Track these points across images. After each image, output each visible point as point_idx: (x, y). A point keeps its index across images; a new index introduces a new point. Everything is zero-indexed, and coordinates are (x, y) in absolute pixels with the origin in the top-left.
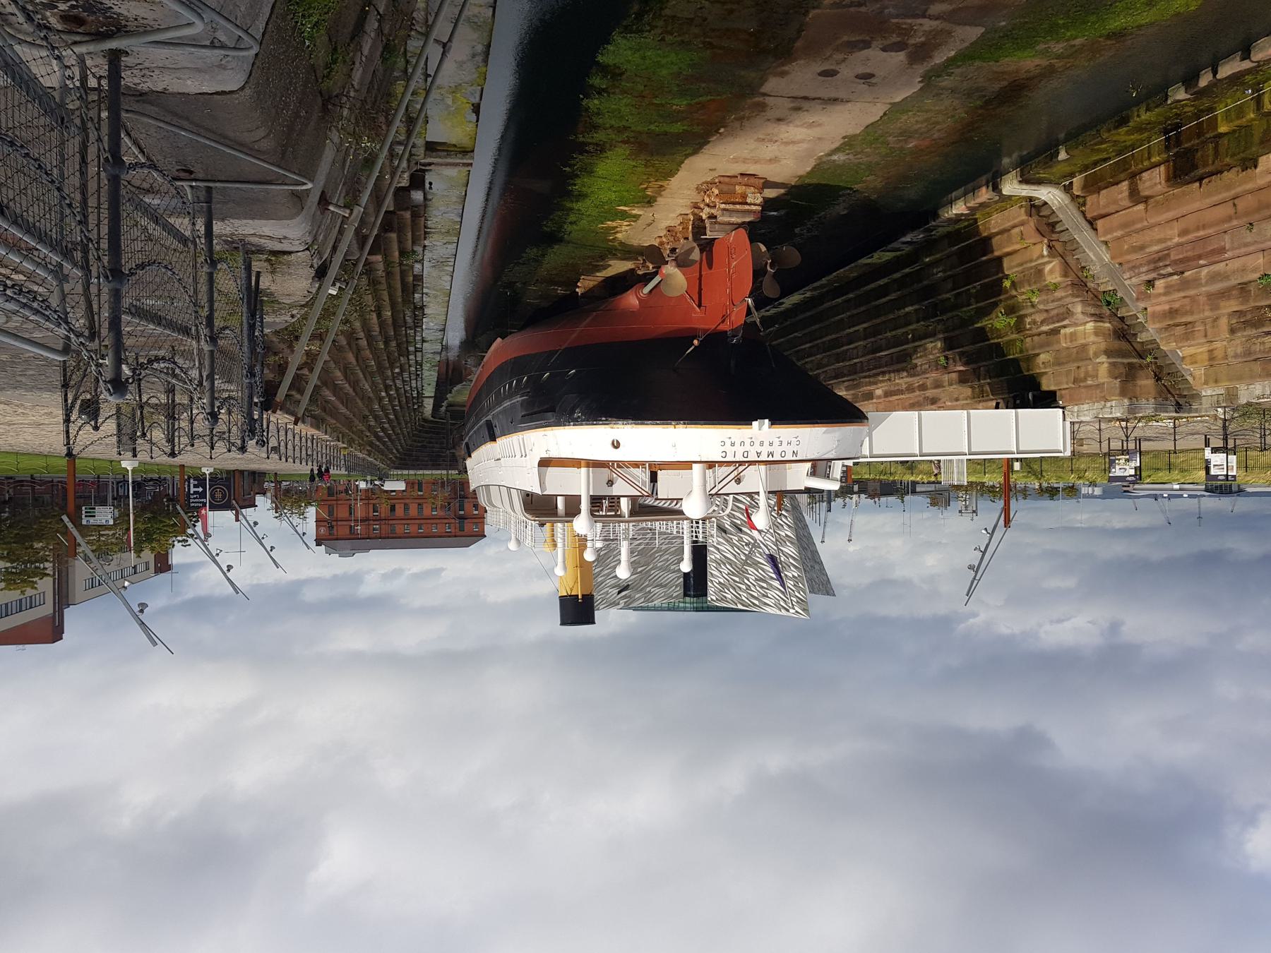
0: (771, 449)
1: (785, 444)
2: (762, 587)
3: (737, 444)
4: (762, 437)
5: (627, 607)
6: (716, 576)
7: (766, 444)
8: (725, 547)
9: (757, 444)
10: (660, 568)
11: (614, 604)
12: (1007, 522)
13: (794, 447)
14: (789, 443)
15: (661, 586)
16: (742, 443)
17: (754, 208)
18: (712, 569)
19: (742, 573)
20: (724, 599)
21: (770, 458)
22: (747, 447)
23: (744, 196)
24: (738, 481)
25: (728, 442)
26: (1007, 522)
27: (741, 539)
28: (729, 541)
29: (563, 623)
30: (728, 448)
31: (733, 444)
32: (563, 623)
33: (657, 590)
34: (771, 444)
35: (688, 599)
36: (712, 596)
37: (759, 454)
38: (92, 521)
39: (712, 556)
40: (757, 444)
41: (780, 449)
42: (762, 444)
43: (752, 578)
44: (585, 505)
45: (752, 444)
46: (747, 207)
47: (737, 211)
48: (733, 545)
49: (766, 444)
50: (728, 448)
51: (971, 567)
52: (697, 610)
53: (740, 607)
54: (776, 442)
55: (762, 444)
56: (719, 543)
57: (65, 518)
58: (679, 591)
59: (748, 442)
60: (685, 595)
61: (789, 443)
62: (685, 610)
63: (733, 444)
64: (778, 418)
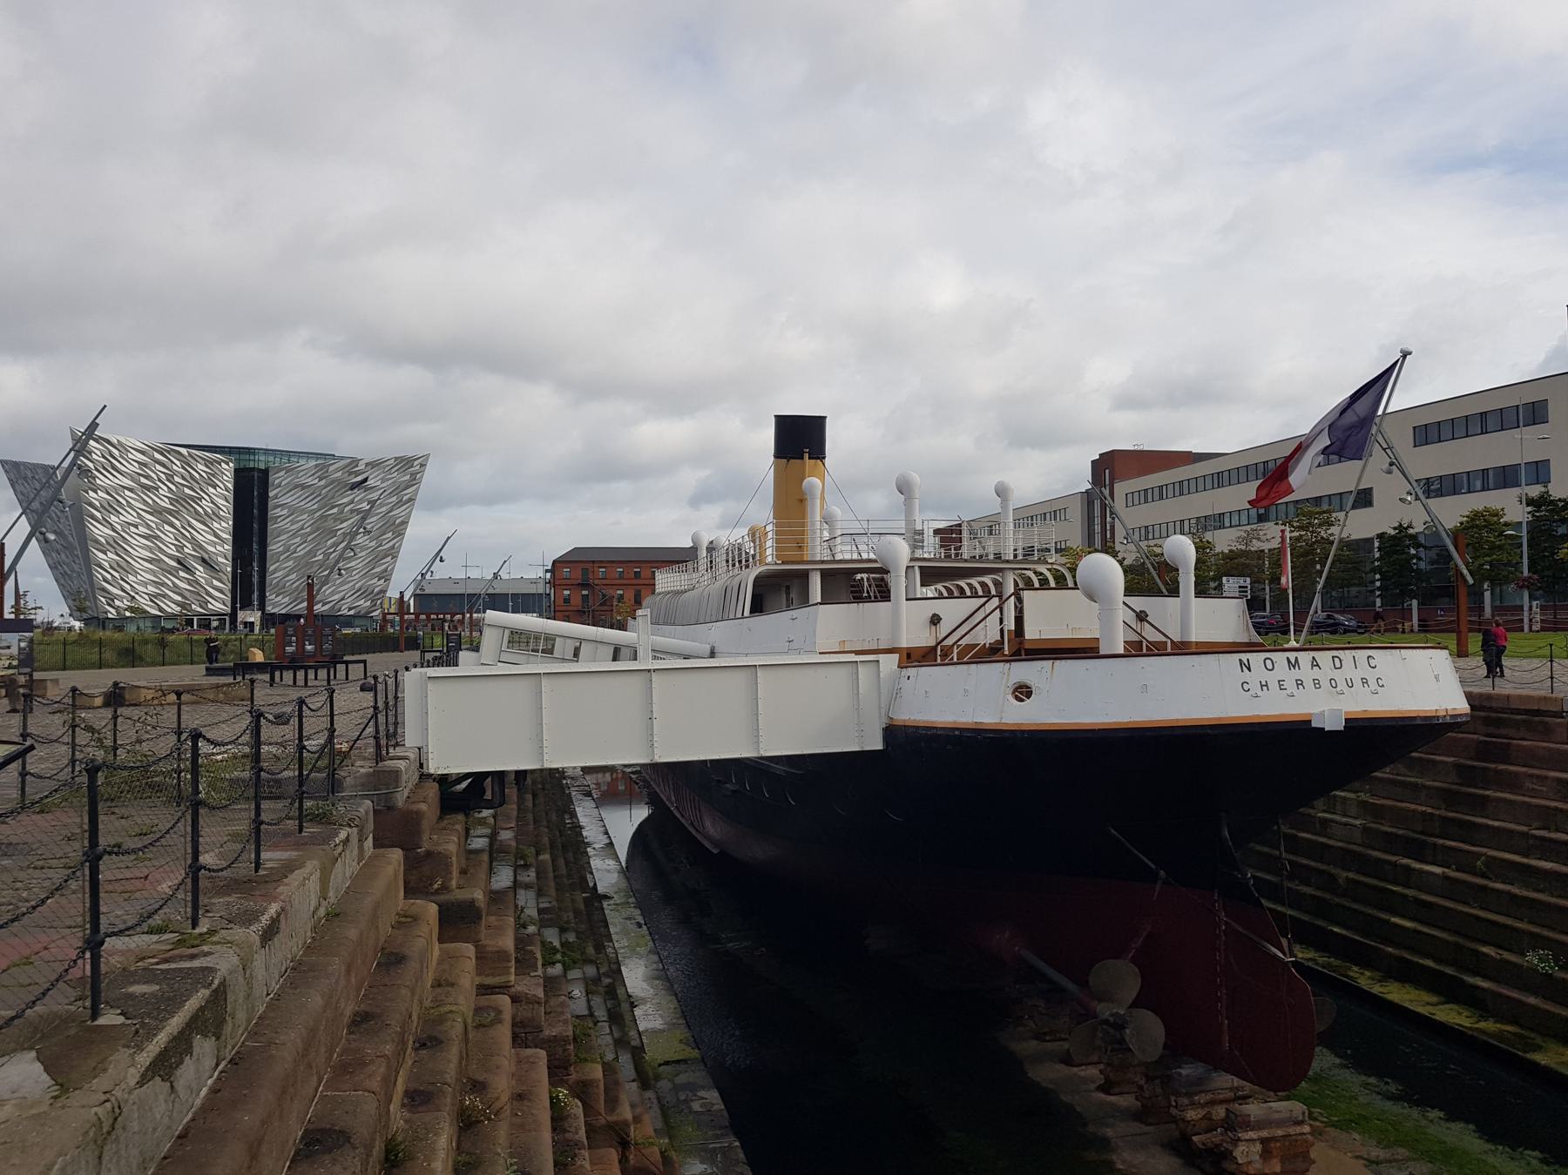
0: (1295, 674)
1: (1273, 685)
3: (1357, 683)
5: (355, 462)
6: (220, 497)
7: (1308, 684)
8: (204, 537)
9: (1325, 684)
10: (303, 512)
11: (372, 465)
15: (303, 487)
17: (1252, 1135)
18: (226, 508)
19: (179, 500)
23: (1266, 1154)
24: (935, 620)
27: (180, 548)
28: (197, 545)
29: (820, 421)
31: (1364, 681)
32: (820, 421)
33: (310, 481)
34: (1299, 683)
35: (262, 466)
36: (227, 470)
37: (1315, 664)
38: (1241, 581)
39: (225, 527)
40: (1325, 684)
43: (164, 491)
44: (1188, 581)
46: (1265, 1134)
47: (1280, 1123)
49: (1308, 684)
50: (1371, 676)
52: (249, 451)
54: (1290, 685)
56: (214, 544)
57: (1471, 581)
58: (276, 478)
59: (1342, 686)
60: (265, 473)
62: (267, 451)
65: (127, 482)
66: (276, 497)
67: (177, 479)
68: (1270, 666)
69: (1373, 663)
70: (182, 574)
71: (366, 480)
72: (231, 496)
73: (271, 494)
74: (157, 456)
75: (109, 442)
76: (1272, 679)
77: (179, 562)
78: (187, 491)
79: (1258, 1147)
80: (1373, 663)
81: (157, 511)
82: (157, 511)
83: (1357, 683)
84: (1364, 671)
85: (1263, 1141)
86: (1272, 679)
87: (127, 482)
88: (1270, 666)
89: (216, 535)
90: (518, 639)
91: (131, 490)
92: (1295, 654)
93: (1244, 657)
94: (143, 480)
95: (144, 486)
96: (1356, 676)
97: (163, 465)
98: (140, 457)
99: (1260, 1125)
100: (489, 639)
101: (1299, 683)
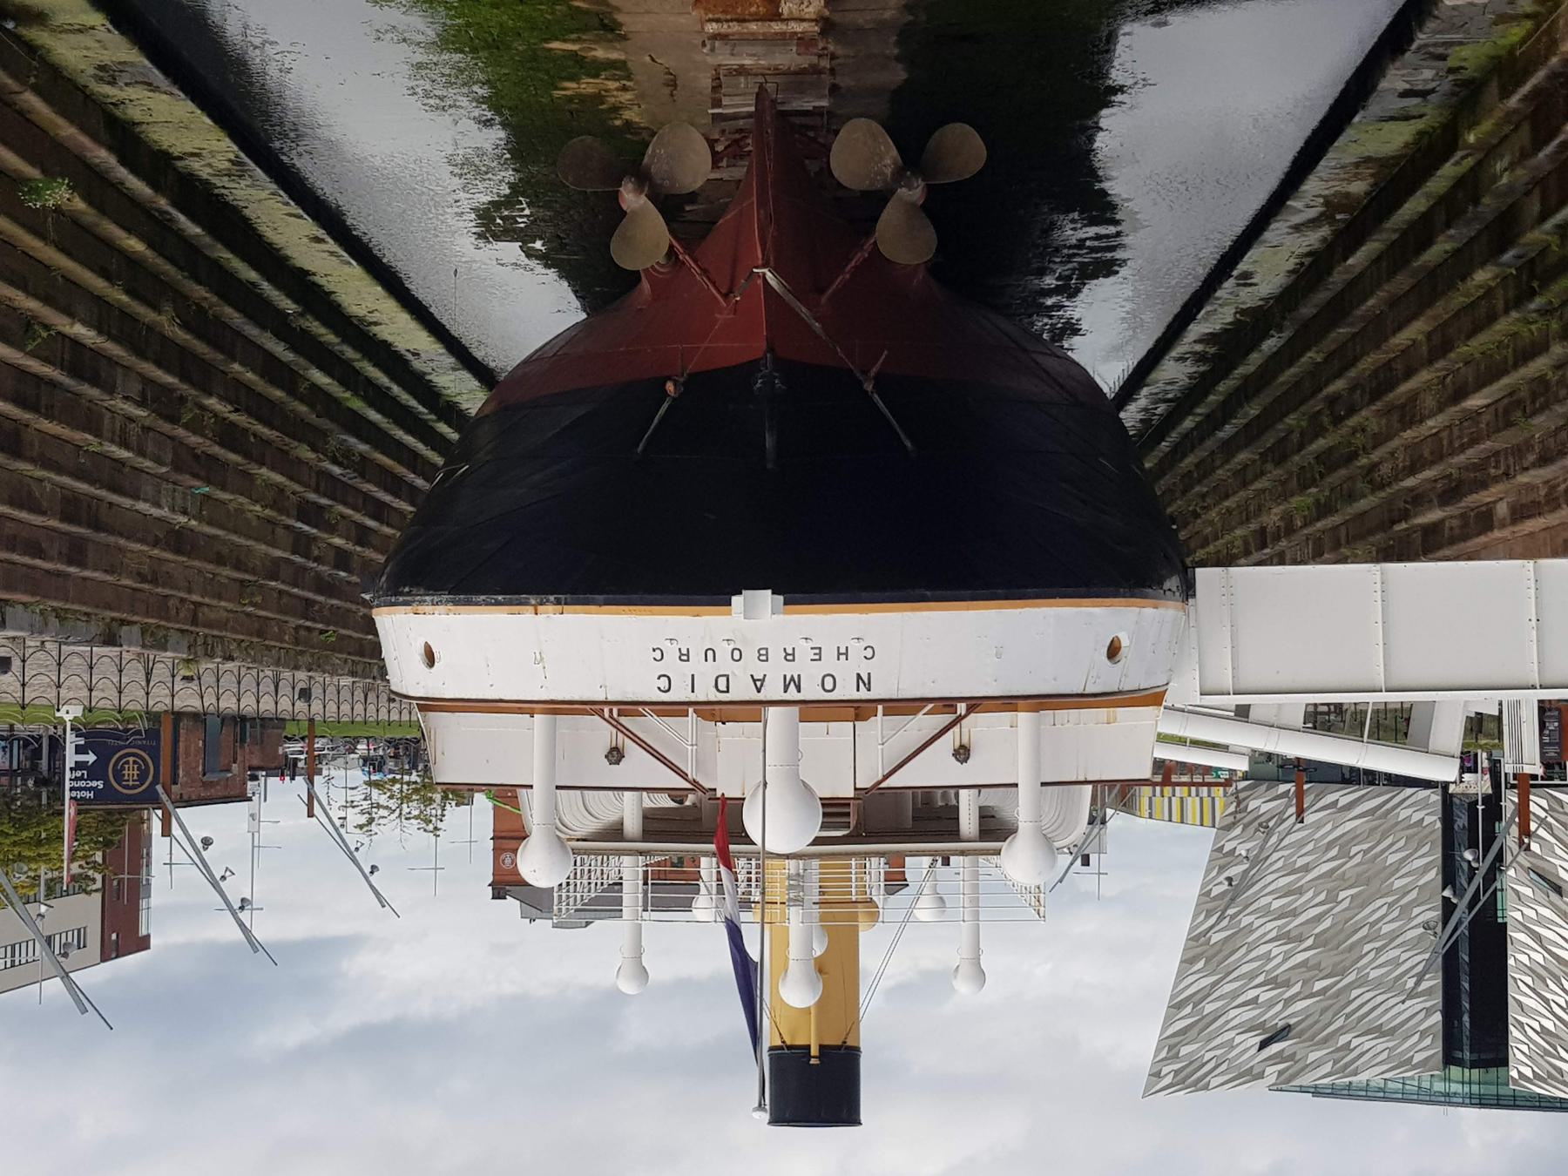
0: (791, 670)
1: (829, 654)
3: (697, 656)
4: (755, 635)
7: (776, 655)
9: (750, 655)
14: (843, 654)
16: (710, 654)
21: (792, 694)
22: (724, 664)
25: (671, 652)
30: (671, 665)
34: (790, 656)
37: (759, 684)
40: (750, 655)
41: (819, 669)
42: (763, 655)
45: (737, 655)
49: (776, 655)
50: (671, 665)
54: (804, 652)
55: (763, 655)
59: (724, 651)
61: (843, 654)
63: (685, 657)
64: (805, 584)
68: (829, 681)
69: (663, 683)
76: (829, 663)
83: (697, 656)
84: (680, 673)
86: (829, 663)
88: (829, 681)
90: (1395, 726)
92: (787, 697)
93: (863, 694)
96: (696, 664)
101: (790, 656)
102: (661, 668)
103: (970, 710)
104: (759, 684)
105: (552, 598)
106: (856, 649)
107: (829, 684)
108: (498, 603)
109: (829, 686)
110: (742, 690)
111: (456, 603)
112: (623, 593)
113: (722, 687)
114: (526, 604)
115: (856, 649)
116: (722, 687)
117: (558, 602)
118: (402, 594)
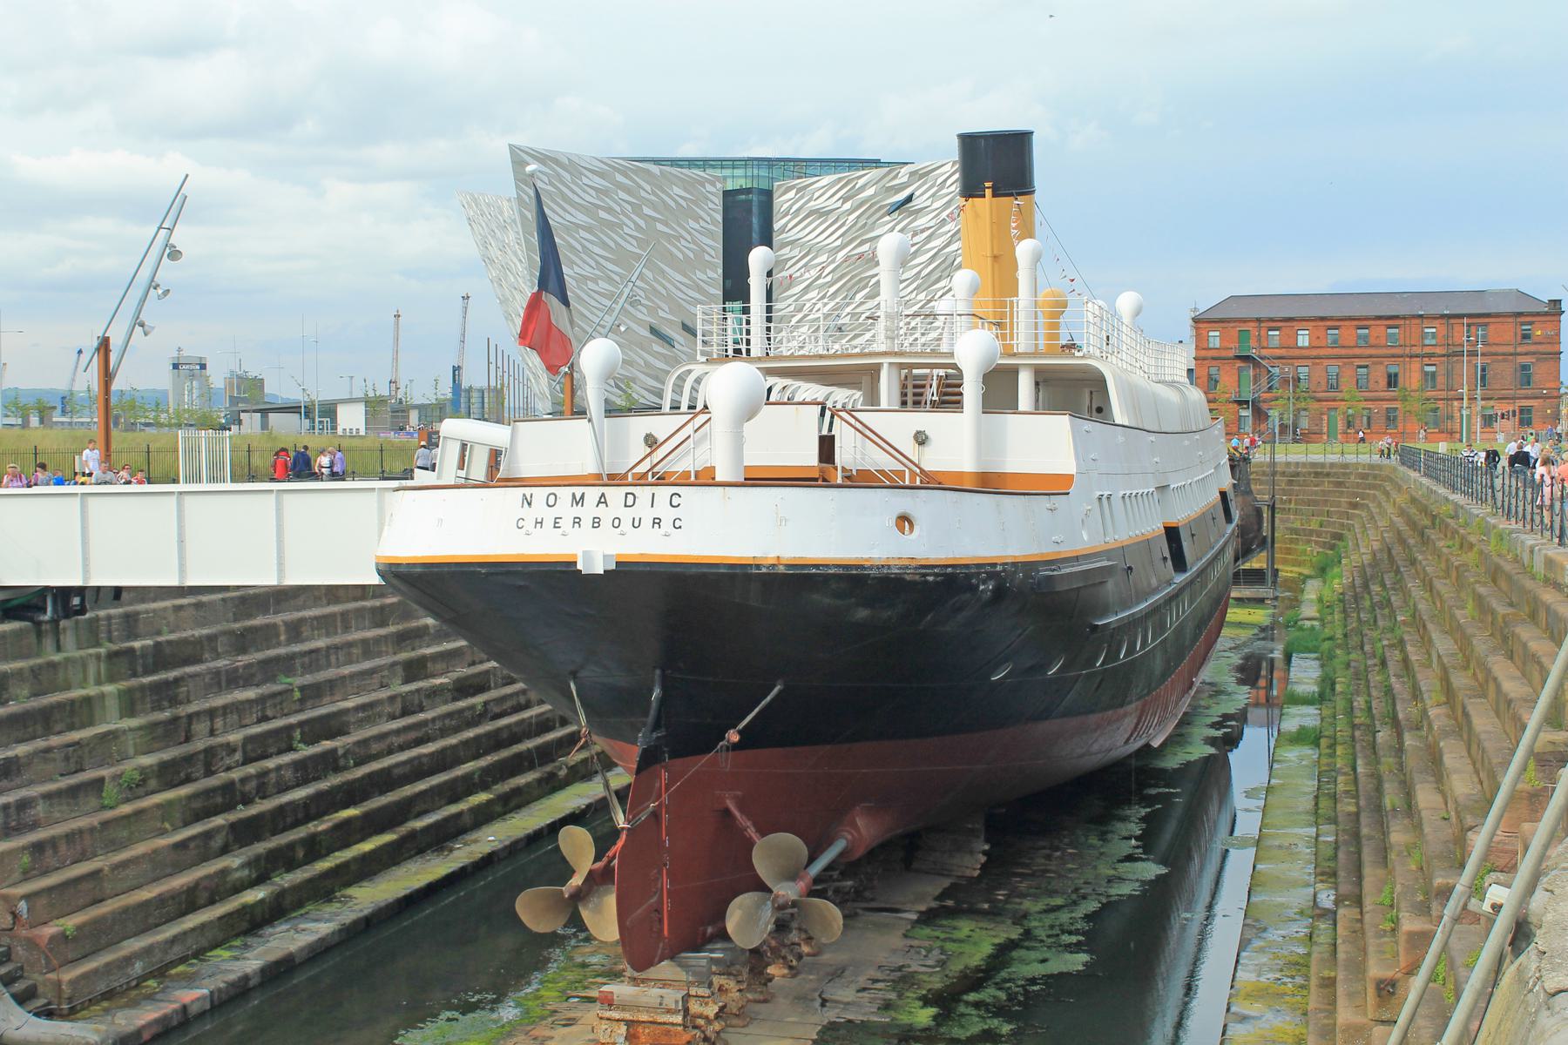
0: (577, 511)
1: (548, 523)
2: (609, 210)
7: (587, 523)
12: (104, 346)
13: (530, 514)
15: (821, 213)
20: (688, 185)
21: (578, 491)
22: (627, 515)
25: (667, 524)
26: (104, 346)
27: (653, 311)
30: (667, 514)
33: (832, 204)
34: (577, 521)
37: (602, 500)
40: (606, 523)
42: (596, 523)
44: (971, 391)
46: (628, 1016)
48: (669, 298)
50: (667, 514)
51: (175, 254)
53: (655, 169)
54: (566, 524)
55: (596, 523)
58: (782, 201)
59: (626, 525)
63: (657, 522)
64: (556, 579)
65: (581, 218)
66: (783, 230)
67: (646, 211)
69: (676, 501)
70: (656, 348)
71: (909, 199)
72: (719, 230)
73: (776, 226)
74: (619, 178)
75: (557, 162)
77: (653, 331)
78: (660, 227)
79: (623, 1029)
80: (676, 501)
81: (623, 259)
82: (623, 259)
85: (629, 1023)
87: (581, 218)
89: (699, 290)
91: (588, 229)
94: (603, 214)
95: (603, 222)
97: (628, 191)
98: (598, 182)
99: (623, 1007)
100: (448, 455)
101: (577, 521)
102: (675, 513)
103: (625, 476)
104: (602, 500)
105: (764, 570)
106: (529, 525)
107: (630, 499)
108: (816, 566)
109: (552, 498)
110: (615, 494)
111: (862, 567)
112: (704, 575)
113: (630, 498)
114: (789, 566)
115: (529, 525)
116: (630, 498)
117: (758, 566)
118: (936, 575)
